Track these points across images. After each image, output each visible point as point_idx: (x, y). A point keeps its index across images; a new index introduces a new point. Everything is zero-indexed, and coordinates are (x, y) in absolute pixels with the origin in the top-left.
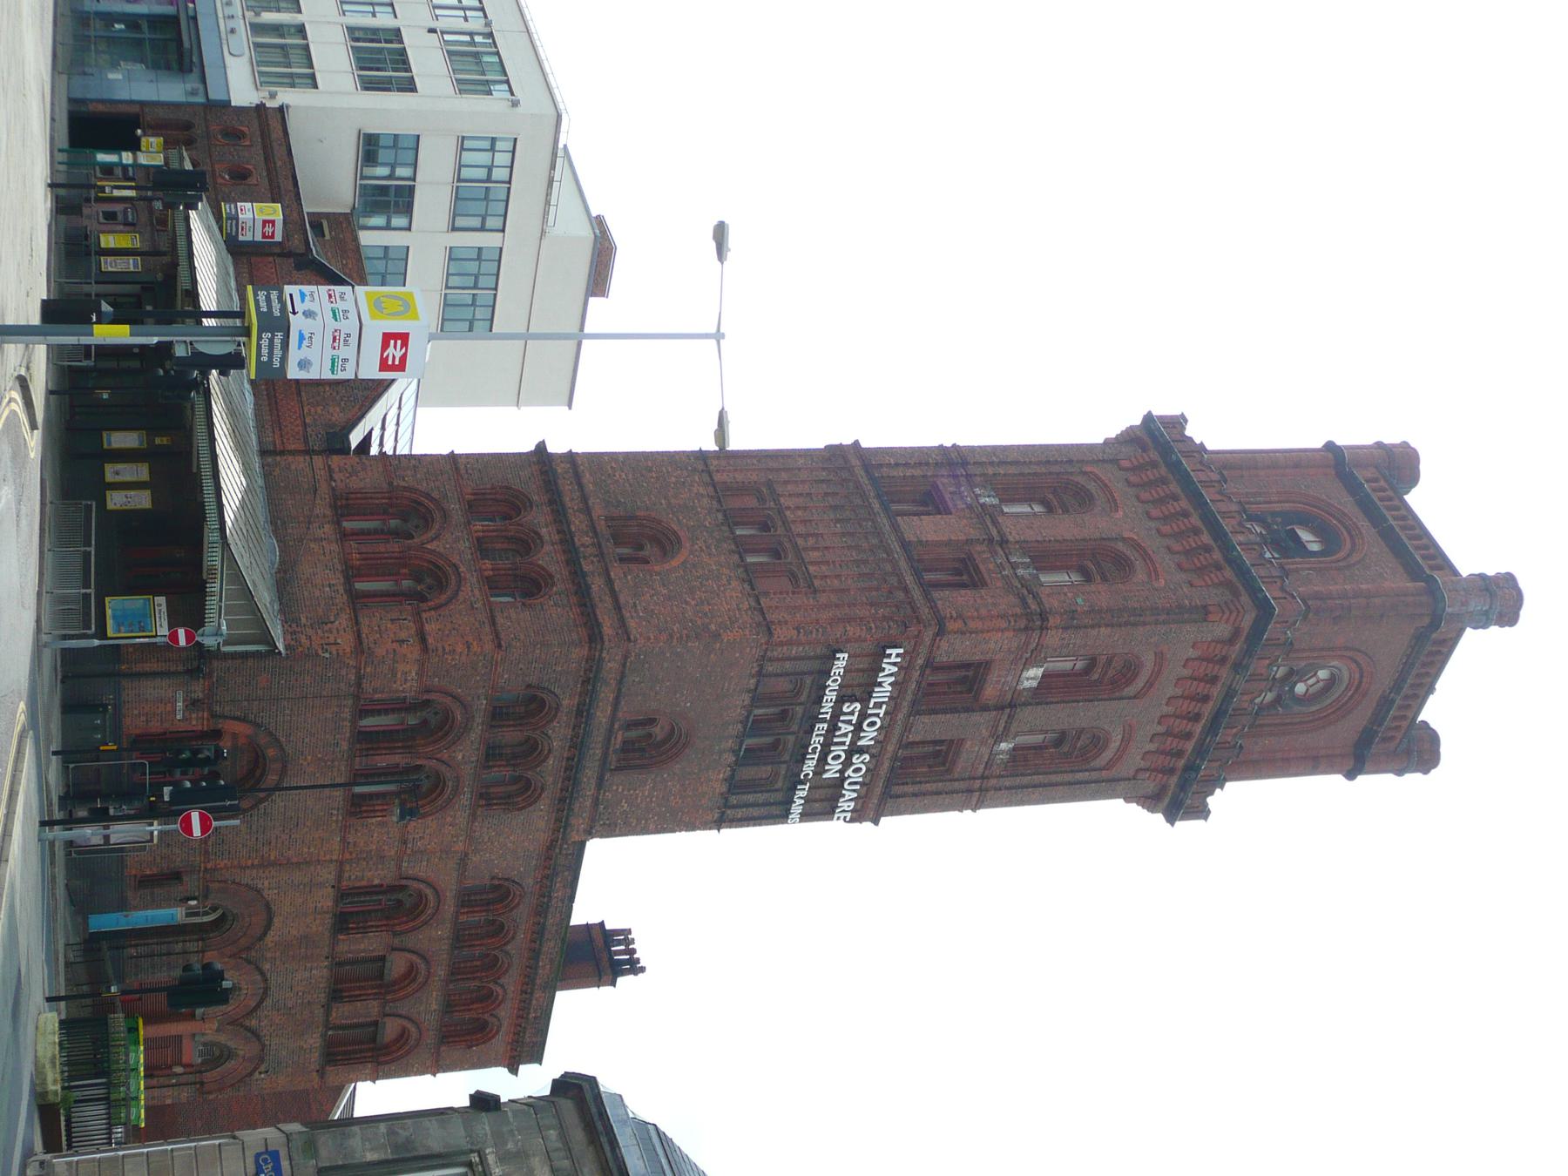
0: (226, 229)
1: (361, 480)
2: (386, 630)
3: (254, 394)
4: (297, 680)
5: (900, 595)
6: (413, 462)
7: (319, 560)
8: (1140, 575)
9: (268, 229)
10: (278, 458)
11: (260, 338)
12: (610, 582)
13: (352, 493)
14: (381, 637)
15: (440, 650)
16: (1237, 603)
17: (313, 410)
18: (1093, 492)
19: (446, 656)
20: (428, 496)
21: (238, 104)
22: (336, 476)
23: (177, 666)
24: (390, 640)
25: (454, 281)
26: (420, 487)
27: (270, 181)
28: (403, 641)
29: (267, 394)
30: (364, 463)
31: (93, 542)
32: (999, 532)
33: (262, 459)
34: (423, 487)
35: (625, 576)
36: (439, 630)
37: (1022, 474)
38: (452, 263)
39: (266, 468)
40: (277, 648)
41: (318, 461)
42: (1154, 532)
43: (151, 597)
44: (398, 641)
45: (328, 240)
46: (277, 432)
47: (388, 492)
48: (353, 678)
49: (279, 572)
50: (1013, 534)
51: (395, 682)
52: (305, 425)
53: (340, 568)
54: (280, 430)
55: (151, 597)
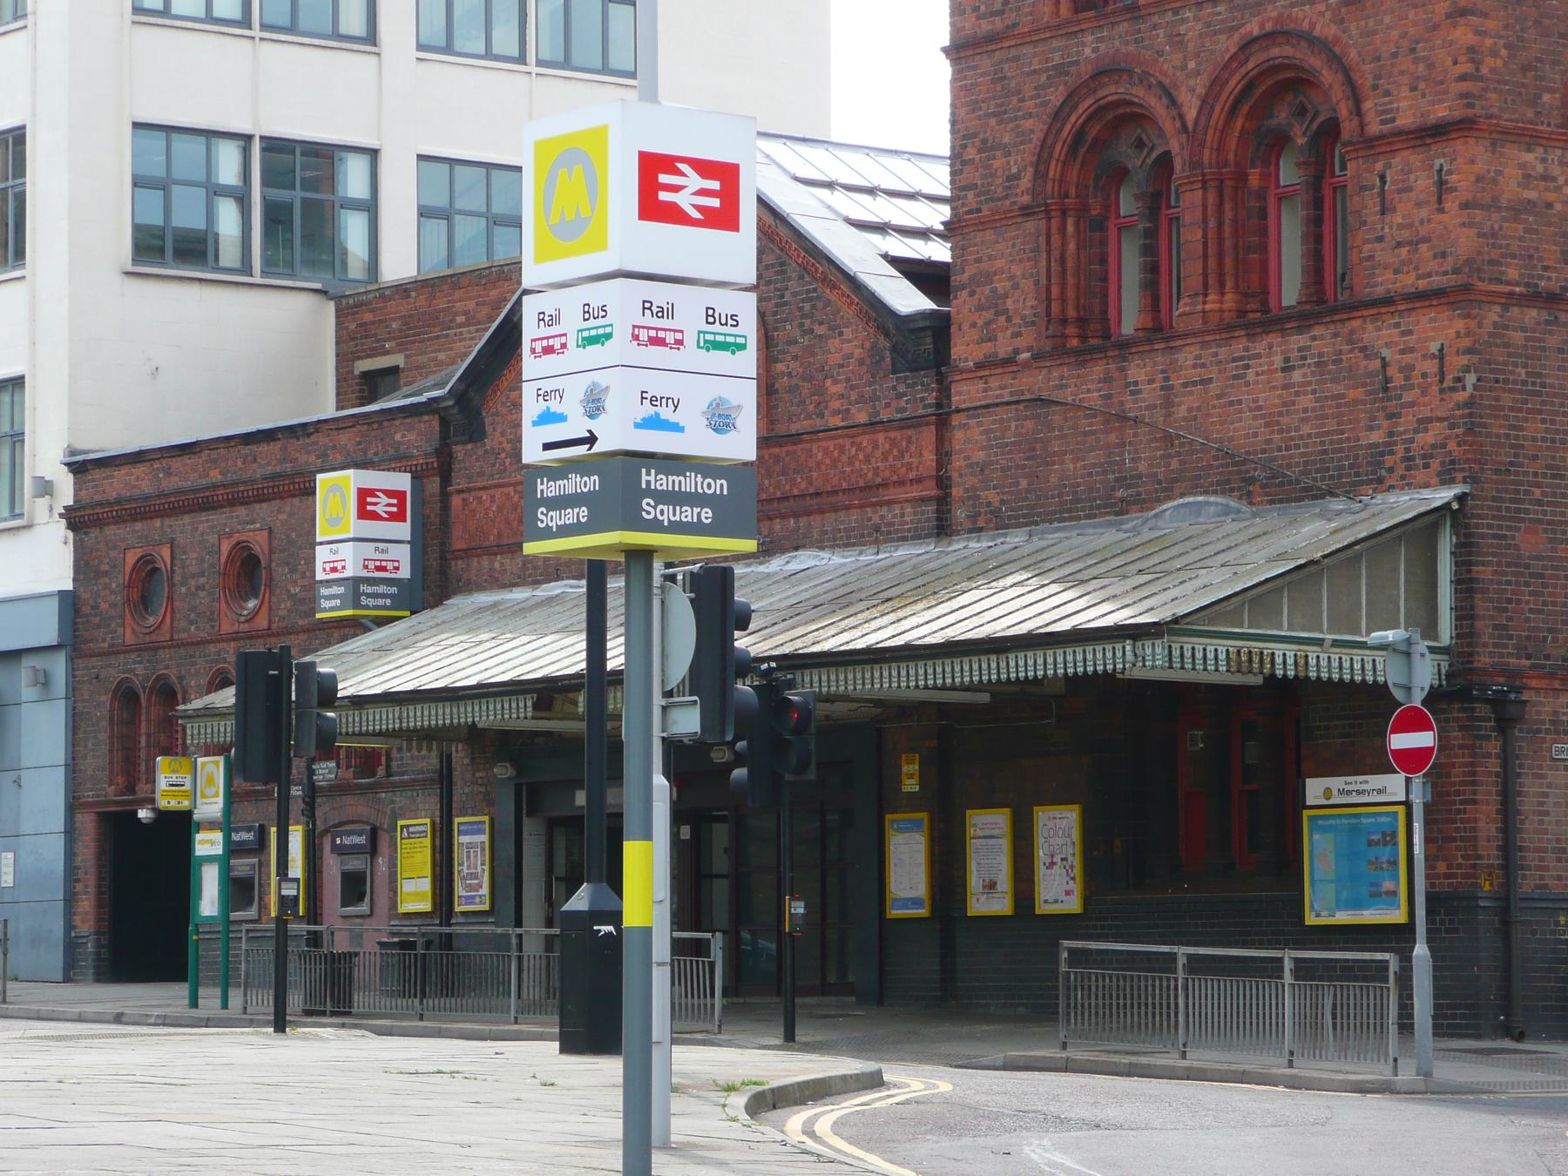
0: (384, 607)
1: (1016, 287)
2: (1411, 225)
3: (796, 549)
4: (1535, 457)
6: (971, 153)
7: (1219, 397)
9: (382, 505)
10: (956, 492)
11: (655, 526)
13: (1049, 307)
14: (1427, 240)
15: (1466, 86)
17: (835, 405)
19: (1485, 71)
20: (1058, 116)
21: (70, 573)
22: (1003, 350)
23: (1489, 755)
24: (1440, 217)
25: (505, 40)
26: (1037, 137)
27: (260, 499)
28: (1441, 183)
29: (796, 515)
30: (972, 278)
31: (1165, 949)
33: (958, 533)
34: (1035, 127)
36: (1414, 89)
38: (458, 47)
39: (981, 524)
40: (1448, 504)
41: (964, 393)
43: (1306, 813)
44: (1440, 201)
45: (407, 357)
46: (892, 493)
47: (1049, 219)
48: (1534, 313)
49: (1248, 497)
51: (1550, 206)
52: (873, 425)
53: (1244, 342)
54: (885, 485)
55: (1306, 813)
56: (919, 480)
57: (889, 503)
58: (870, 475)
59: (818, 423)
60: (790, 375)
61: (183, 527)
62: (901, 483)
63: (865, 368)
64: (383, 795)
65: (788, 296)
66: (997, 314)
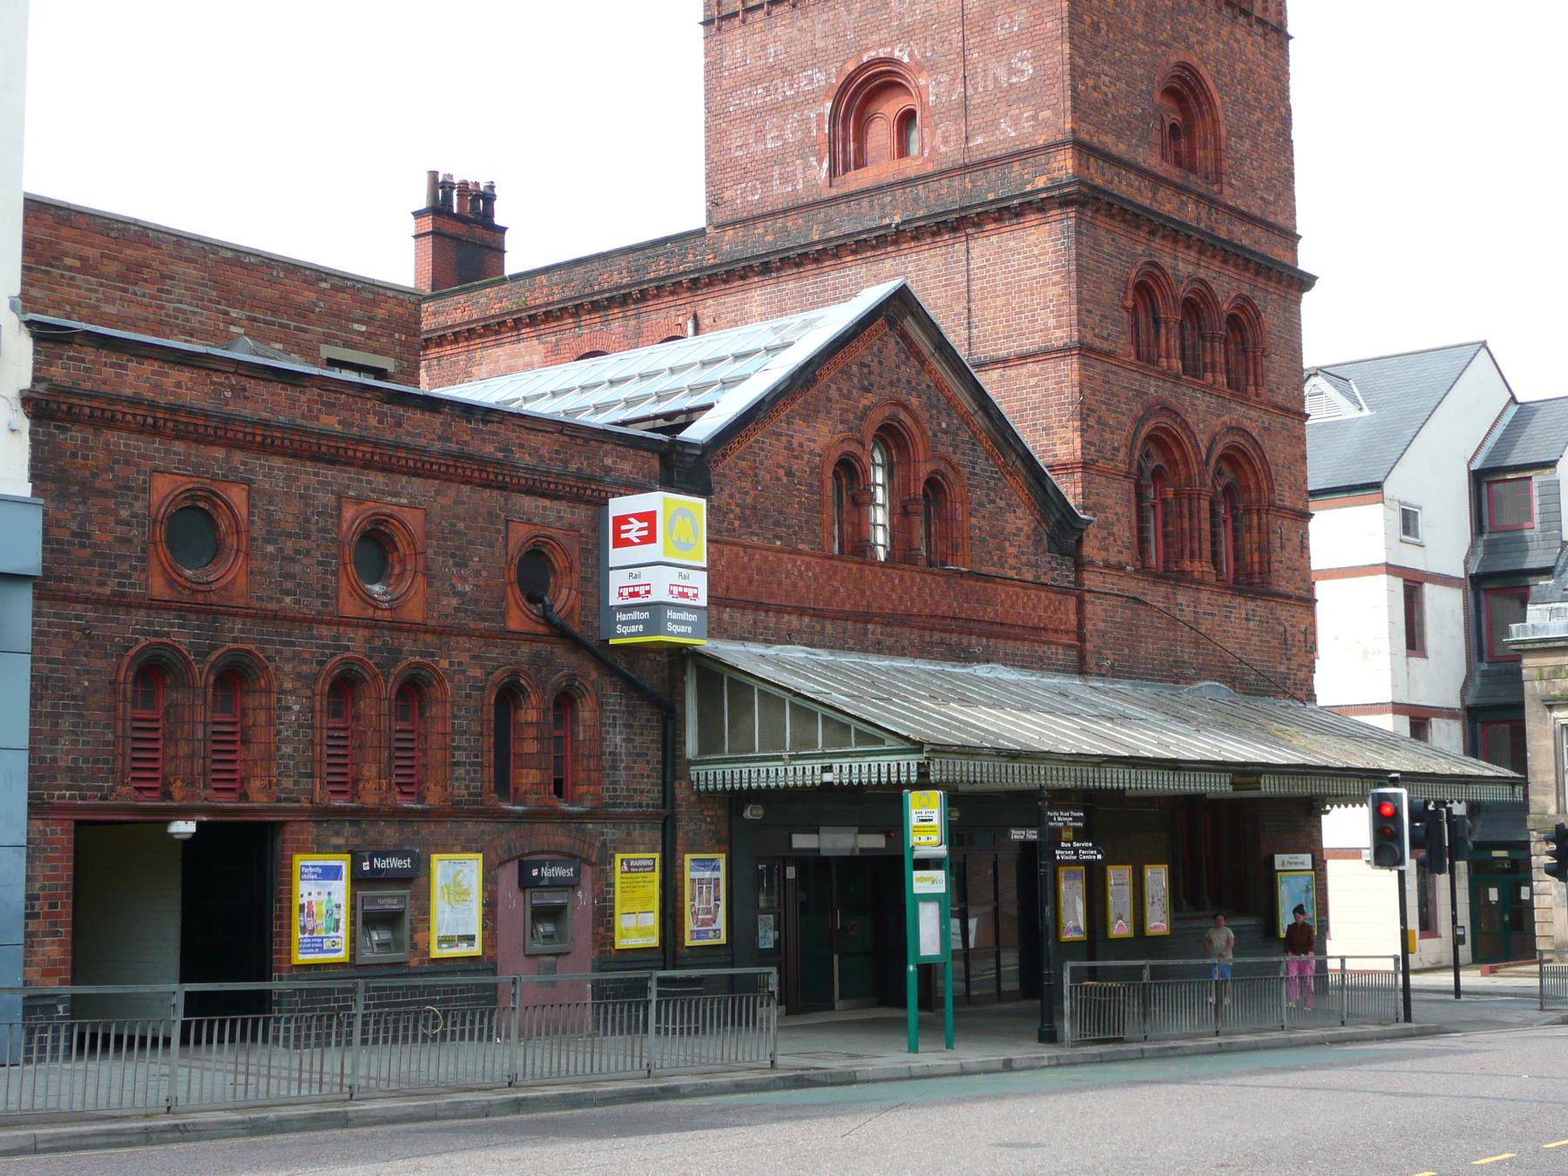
1: (1118, 520)
7: (1220, 625)
9: (634, 530)
27: (421, 472)
29: (989, 637)
33: (1091, 674)
41: (1091, 580)
46: (1051, 636)
54: (1045, 629)
56: (1067, 632)
57: (1050, 643)
58: (1036, 620)
59: (1001, 572)
60: (980, 529)
61: (272, 472)
62: (1056, 631)
63: (1030, 543)
64: (591, 826)
65: (978, 468)
66: (1110, 534)
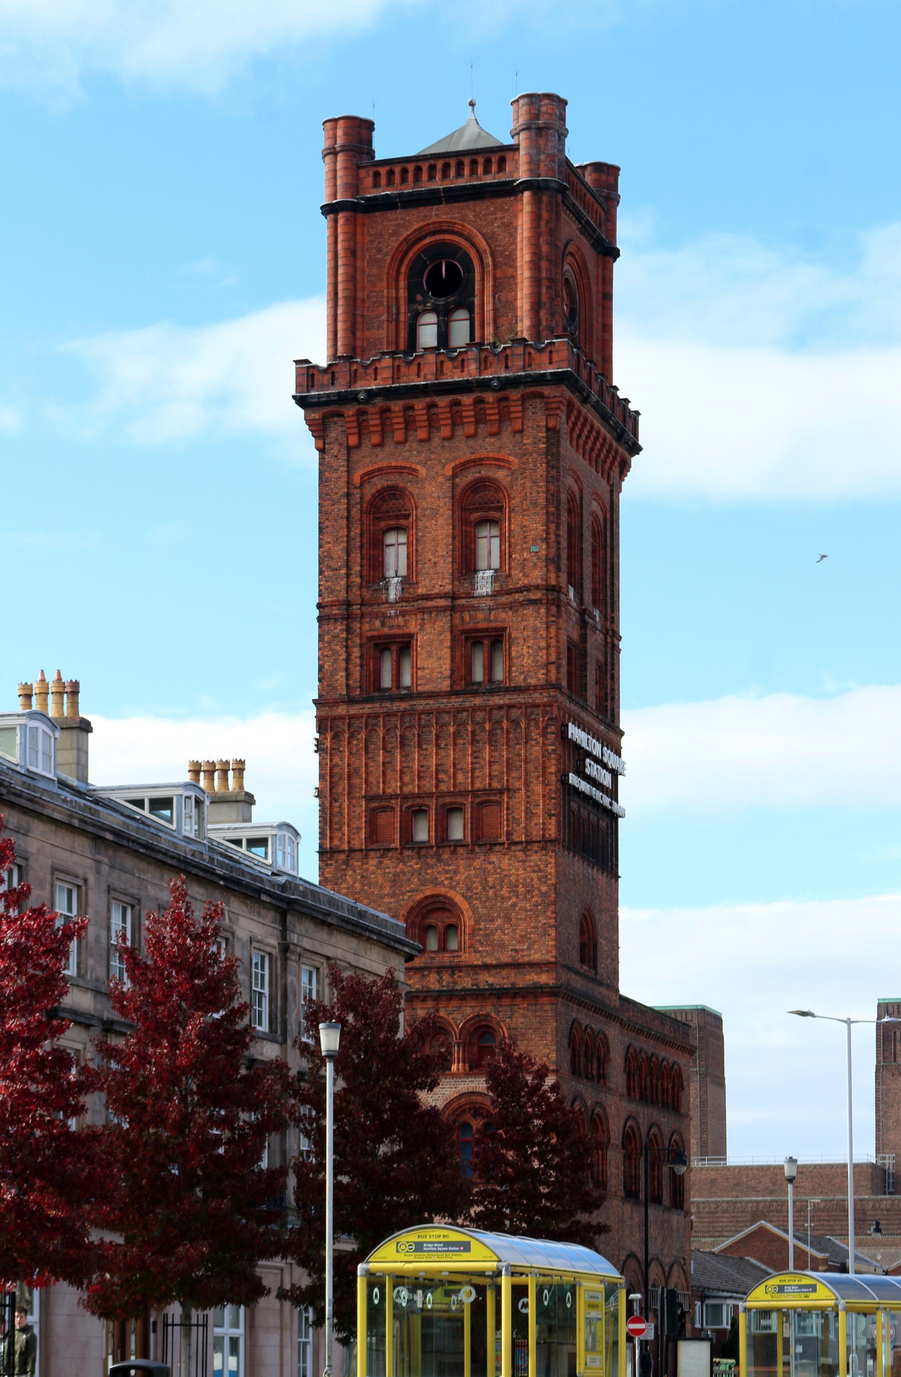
5: (515, 713)
8: (501, 475)
12: (486, 967)
16: (551, 400)
18: (385, 484)
32: (441, 598)
35: (480, 952)
37: (362, 547)
42: (446, 444)
50: (444, 584)
